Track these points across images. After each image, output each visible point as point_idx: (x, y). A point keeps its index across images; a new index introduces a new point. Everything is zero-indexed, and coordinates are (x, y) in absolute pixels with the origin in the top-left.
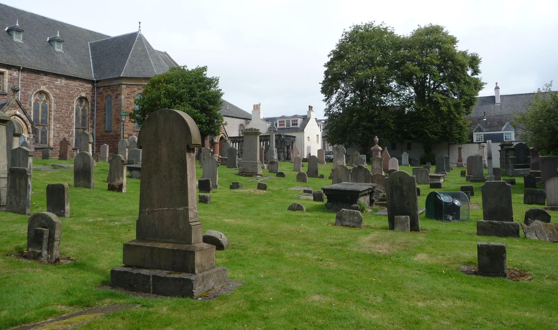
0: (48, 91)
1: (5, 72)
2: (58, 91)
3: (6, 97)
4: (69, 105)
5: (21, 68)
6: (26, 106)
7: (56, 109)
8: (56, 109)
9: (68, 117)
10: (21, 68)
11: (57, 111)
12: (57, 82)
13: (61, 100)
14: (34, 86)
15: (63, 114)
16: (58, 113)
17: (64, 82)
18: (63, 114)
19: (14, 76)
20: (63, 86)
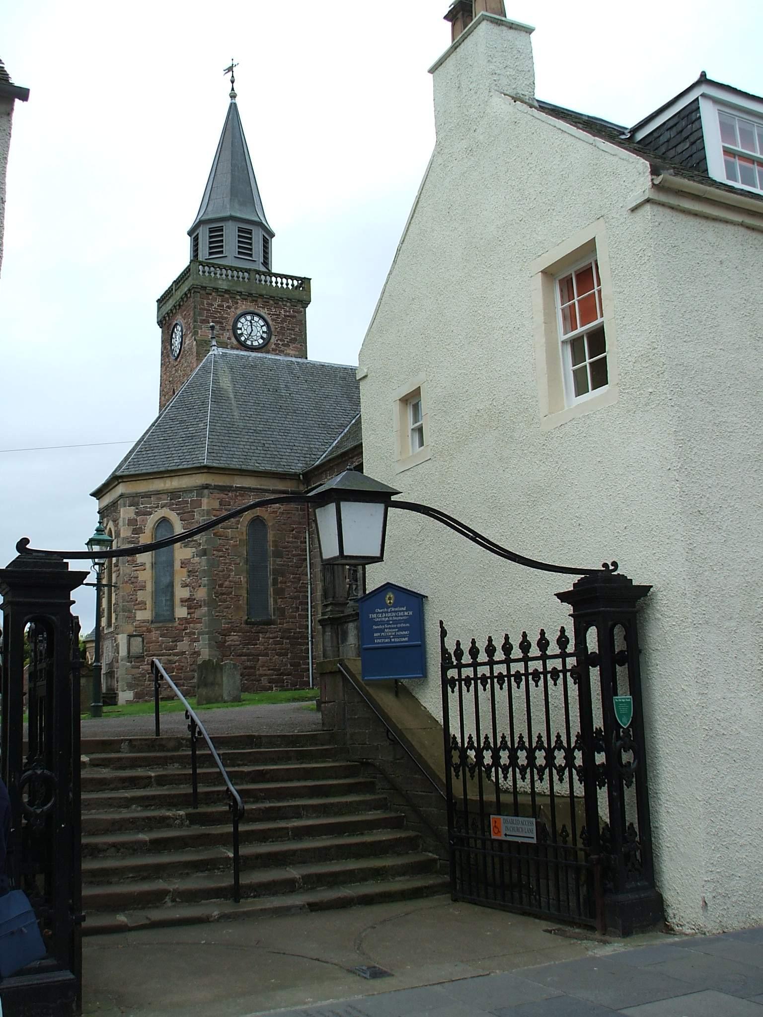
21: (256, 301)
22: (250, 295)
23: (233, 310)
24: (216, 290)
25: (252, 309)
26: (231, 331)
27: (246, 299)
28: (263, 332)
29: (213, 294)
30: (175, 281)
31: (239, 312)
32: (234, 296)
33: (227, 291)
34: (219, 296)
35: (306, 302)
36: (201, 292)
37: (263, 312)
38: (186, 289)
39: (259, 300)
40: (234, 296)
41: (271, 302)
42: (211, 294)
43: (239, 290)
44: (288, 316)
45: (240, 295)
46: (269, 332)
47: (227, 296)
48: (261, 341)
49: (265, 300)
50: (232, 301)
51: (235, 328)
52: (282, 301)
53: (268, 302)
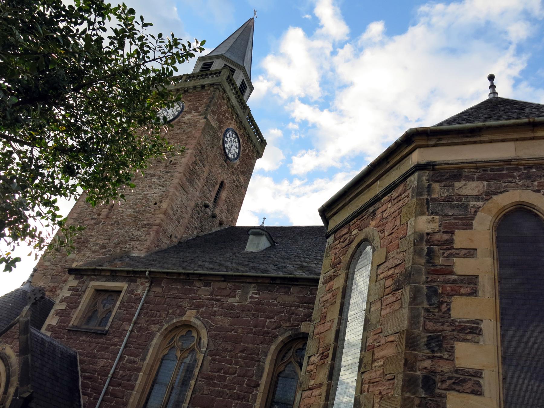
1: (123, 287)
2: (226, 322)
4: (253, 359)
5: (147, 272)
6: (134, 362)
9: (238, 399)
10: (147, 272)
11: (209, 378)
12: (231, 300)
15: (226, 386)
17: (251, 297)
18: (226, 386)
19: (136, 295)
20: (243, 308)
21: (241, 129)
22: (241, 122)
23: (229, 121)
24: (229, 100)
25: (237, 132)
26: (222, 134)
27: (237, 123)
29: (225, 101)
30: (187, 75)
32: (234, 114)
33: (233, 107)
34: (227, 105)
35: (259, 155)
36: (221, 93)
37: (241, 140)
38: (207, 83)
39: (242, 131)
40: (234, 114)
41: (246, 138)
42: (224, 100)
43: (239, 112)
45: (236, 117)
46: (238, 154)
47: (230, 110)
48: (233, 157)
49: (245, 133)
50: (231, 116)
51: (225, 135)
52: (251, 143)
53: (245, 136)
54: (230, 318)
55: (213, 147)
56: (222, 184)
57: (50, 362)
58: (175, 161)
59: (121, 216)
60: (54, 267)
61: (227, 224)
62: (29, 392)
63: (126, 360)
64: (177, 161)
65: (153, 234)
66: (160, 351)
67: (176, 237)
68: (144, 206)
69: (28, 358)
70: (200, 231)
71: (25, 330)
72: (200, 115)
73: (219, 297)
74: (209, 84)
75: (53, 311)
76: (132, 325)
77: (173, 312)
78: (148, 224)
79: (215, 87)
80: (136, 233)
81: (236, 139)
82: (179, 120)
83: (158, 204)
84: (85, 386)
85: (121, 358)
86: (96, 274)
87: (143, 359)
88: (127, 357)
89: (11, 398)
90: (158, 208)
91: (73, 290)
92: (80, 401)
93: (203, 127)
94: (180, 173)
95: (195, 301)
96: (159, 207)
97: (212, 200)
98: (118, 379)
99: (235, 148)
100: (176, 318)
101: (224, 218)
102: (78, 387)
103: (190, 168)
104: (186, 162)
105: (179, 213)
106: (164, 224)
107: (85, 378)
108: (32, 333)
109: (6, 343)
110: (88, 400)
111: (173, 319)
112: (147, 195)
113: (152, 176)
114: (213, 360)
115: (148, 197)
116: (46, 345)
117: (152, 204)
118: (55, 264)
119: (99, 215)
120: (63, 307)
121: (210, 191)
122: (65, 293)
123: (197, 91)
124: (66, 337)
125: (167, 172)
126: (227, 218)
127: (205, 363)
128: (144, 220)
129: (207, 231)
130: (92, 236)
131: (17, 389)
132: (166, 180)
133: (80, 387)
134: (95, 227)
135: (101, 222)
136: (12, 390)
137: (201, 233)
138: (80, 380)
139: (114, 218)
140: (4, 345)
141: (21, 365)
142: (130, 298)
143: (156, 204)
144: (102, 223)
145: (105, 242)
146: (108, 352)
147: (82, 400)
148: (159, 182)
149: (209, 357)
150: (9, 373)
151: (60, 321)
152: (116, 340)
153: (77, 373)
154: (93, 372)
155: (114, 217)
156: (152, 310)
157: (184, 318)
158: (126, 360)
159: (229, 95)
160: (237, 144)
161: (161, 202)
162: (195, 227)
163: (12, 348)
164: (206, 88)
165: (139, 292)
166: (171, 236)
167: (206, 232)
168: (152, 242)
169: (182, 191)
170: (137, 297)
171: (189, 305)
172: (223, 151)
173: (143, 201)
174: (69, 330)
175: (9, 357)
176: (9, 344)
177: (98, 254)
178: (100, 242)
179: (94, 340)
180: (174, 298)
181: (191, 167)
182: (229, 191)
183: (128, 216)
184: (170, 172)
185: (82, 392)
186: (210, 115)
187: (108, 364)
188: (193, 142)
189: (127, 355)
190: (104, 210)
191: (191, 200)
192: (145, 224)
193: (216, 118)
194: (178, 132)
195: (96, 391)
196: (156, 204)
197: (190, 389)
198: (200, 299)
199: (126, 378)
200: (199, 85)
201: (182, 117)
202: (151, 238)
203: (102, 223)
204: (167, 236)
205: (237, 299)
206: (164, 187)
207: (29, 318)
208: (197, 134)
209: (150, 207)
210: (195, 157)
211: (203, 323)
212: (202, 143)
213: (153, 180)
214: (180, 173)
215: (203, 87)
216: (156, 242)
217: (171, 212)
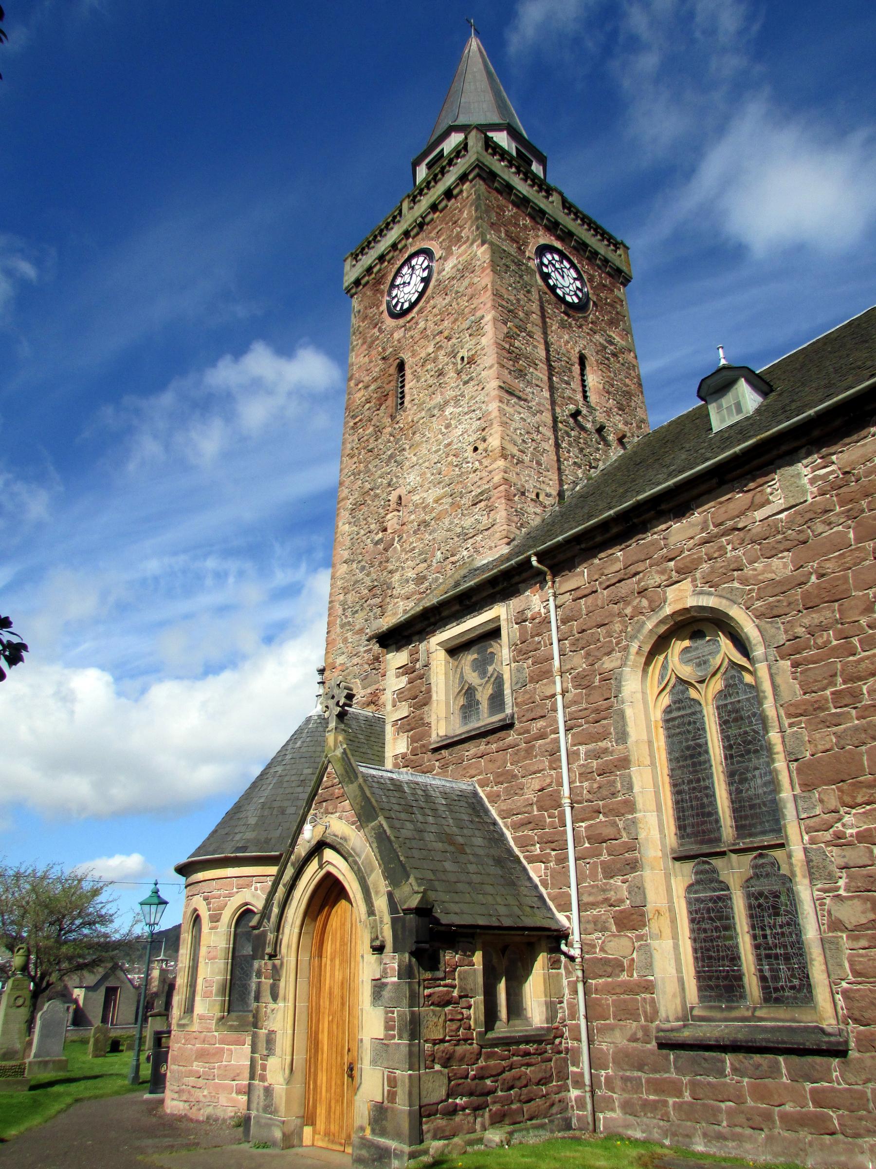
0: (710, 602)
1: (498, 618)
3: (512, 737)
6: (605, 751)
7: (799, 696)
8: (799, 696)
13: (826, 614)
14: (628, 611)
16: (826, 723)
17: (812, 481)
25: (558, 245)
28: (577, 288)
31: (542, 241)
44: (604, 286)
48: (576, 301)
54: (786, 554)
55: (529, 292)
56: (582, 360)
57: (431, 819)
58: (470, 353)
59: (424, 508)
60: (356, 660)
61: (633, 436)
62: (418, 893)
63: (582, 756)
64: (473, 352)
65: (501, 505)
66: (651, 705)
67: (548, 495)
68: (456, 466)
69: (381, 825)
70: (588, 467)
71: (350, 774)
72: (472, 244)
73: (731, 523)
74: (456, 180)
75: (389, 730)
76: (558, 679)
77: (635, 608)
78: (481, 493)
79: (470, 177)
80: (468, 522)
81: (565, 263)
82: (437, 280)
83: (481, 447)
84: (524, 844)
85: (572, 756)
86: (432, 620)
87: (623, 737)
88: (582, 749)
89: (387, 919)
90: (484, 454)
91: (403, 674)
92: (530, 879)
93: (487, 261)
94: (491, 367)
95: (672, 563)
96: (486, 450)
97: (579, 397)
98: (588, 801)
99: (572, 281)
100: (649, 618)
101: (620, 426)
102: (510, 851)
103: (504, 349)
104: (492, 341)
105: (531, 446)
106: (512, 477)
107: (516, 827)
108: (365, 777)
109: (327, 812)
110: (546, 868)
111: (644, 623)
112: (449, 444)
113: (442, 407)
114: (795, 665)
115: (455, 447)
116: (406, 789)
117: (469, 453)
118: (354, 653)
119: (385, 530)
120: (404, 710)
121: (568, 383)
122: (395, 683)
123: (441, 212)
124: (437, 764)
125: (466, 383)
126: (626, 423)
127: (779, 680)
128: (469, 490)
129: (601, 463)
130: (391, 572)
131: (390, 895)
132: (472, 396)
133: (516, 850)
134: (390, 553)
135: (393, 539)
136: (381, 903)
137: (592, 470)
138: (508, 834)
139: (414, 520)
140: (326, 820)
141: (375, 845)
142: (523, 631)
143: (476, 449)
144: (397, 539)
145: (420, 570)
146: (536, 757)
147: (532, 874)
148: (461, 409)
149: (782, 663)
150: (359, 869)
151: (413, 740)
152: (541, 723)
153: (495, 823)
154: (526, 809)
155: (413, 517)
156: (584, 631)
157: (668, 610)
158: (582, 756)
159: (506, 177)
160: (572, 271)
161: (484, 440)
162: (575, 463)
163: (340, 818)
164: (455, 192)
165: (537, 610)
166: (538, 495)
167: (601, 466)
168: (509, 521)
169: (514, 400)
170: (537, 621)
171: (664, 578)
172: (552, 296)
173: (449, 459)
174: (436, 750)
175: (345, 839)
176: (332, 813)
177: (418, 596)
178: (411, 574)
179: (494, 747)
180: (619, 581)
181: (507, 346)
182: (604, 369)
183: (436, 501)
184: (471, 379)
185: (526, 857)
186: (490, 234)
187: (548, 781)
188: (487, 298)
189: (581, 744)
190: (389, 517)
191: (541, 412)
192: (477, 496)
193: (503, 235)
194: (446, 301)
195: (553, 845)
196: (476, 449)
197: (778, 753)
198: (682, 552)
199: (604, 792)
200: (439, 197)
201: (439, 273)
202: (501, 515)
203: (397, 539)
204: (532, 500)
205: (779, 501)
206: (474, 411)
207: (345, 746)
208: (485, 279)
209: (468, 462)
210: (505, 324)
211: (721, 596)
212: (503, 291)
213: (447, 413)
214: (491, 367)
215: (449, 194)
216: (516, 519)
217: (515, 451)
